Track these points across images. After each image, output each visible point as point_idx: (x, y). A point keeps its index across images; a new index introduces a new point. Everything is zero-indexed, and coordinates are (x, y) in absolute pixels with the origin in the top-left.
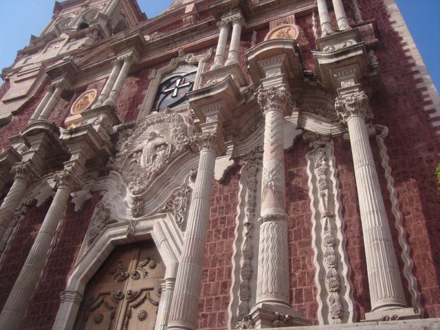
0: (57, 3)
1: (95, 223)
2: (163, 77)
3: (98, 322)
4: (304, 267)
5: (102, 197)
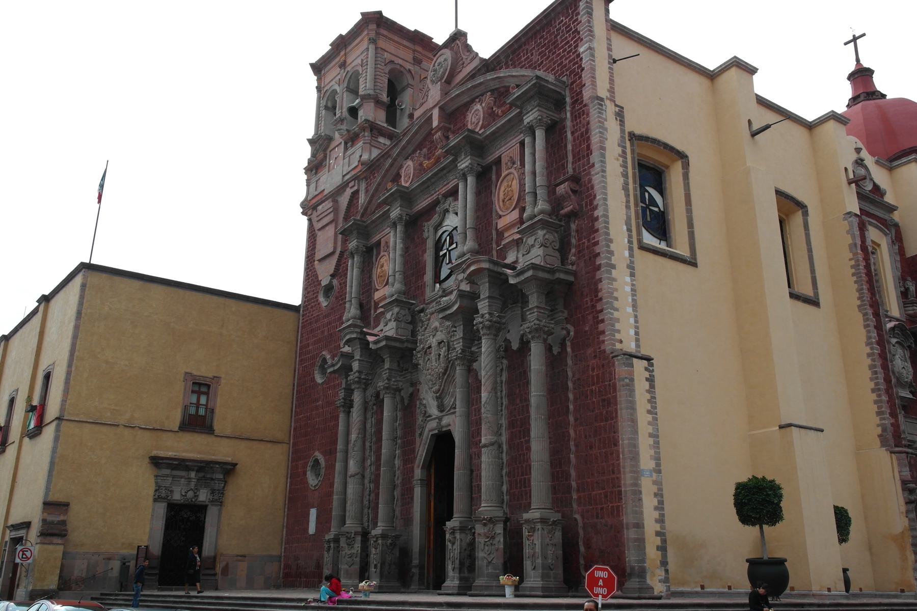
0: (312, 65)
1: (420, 418)
5: (418, 390)
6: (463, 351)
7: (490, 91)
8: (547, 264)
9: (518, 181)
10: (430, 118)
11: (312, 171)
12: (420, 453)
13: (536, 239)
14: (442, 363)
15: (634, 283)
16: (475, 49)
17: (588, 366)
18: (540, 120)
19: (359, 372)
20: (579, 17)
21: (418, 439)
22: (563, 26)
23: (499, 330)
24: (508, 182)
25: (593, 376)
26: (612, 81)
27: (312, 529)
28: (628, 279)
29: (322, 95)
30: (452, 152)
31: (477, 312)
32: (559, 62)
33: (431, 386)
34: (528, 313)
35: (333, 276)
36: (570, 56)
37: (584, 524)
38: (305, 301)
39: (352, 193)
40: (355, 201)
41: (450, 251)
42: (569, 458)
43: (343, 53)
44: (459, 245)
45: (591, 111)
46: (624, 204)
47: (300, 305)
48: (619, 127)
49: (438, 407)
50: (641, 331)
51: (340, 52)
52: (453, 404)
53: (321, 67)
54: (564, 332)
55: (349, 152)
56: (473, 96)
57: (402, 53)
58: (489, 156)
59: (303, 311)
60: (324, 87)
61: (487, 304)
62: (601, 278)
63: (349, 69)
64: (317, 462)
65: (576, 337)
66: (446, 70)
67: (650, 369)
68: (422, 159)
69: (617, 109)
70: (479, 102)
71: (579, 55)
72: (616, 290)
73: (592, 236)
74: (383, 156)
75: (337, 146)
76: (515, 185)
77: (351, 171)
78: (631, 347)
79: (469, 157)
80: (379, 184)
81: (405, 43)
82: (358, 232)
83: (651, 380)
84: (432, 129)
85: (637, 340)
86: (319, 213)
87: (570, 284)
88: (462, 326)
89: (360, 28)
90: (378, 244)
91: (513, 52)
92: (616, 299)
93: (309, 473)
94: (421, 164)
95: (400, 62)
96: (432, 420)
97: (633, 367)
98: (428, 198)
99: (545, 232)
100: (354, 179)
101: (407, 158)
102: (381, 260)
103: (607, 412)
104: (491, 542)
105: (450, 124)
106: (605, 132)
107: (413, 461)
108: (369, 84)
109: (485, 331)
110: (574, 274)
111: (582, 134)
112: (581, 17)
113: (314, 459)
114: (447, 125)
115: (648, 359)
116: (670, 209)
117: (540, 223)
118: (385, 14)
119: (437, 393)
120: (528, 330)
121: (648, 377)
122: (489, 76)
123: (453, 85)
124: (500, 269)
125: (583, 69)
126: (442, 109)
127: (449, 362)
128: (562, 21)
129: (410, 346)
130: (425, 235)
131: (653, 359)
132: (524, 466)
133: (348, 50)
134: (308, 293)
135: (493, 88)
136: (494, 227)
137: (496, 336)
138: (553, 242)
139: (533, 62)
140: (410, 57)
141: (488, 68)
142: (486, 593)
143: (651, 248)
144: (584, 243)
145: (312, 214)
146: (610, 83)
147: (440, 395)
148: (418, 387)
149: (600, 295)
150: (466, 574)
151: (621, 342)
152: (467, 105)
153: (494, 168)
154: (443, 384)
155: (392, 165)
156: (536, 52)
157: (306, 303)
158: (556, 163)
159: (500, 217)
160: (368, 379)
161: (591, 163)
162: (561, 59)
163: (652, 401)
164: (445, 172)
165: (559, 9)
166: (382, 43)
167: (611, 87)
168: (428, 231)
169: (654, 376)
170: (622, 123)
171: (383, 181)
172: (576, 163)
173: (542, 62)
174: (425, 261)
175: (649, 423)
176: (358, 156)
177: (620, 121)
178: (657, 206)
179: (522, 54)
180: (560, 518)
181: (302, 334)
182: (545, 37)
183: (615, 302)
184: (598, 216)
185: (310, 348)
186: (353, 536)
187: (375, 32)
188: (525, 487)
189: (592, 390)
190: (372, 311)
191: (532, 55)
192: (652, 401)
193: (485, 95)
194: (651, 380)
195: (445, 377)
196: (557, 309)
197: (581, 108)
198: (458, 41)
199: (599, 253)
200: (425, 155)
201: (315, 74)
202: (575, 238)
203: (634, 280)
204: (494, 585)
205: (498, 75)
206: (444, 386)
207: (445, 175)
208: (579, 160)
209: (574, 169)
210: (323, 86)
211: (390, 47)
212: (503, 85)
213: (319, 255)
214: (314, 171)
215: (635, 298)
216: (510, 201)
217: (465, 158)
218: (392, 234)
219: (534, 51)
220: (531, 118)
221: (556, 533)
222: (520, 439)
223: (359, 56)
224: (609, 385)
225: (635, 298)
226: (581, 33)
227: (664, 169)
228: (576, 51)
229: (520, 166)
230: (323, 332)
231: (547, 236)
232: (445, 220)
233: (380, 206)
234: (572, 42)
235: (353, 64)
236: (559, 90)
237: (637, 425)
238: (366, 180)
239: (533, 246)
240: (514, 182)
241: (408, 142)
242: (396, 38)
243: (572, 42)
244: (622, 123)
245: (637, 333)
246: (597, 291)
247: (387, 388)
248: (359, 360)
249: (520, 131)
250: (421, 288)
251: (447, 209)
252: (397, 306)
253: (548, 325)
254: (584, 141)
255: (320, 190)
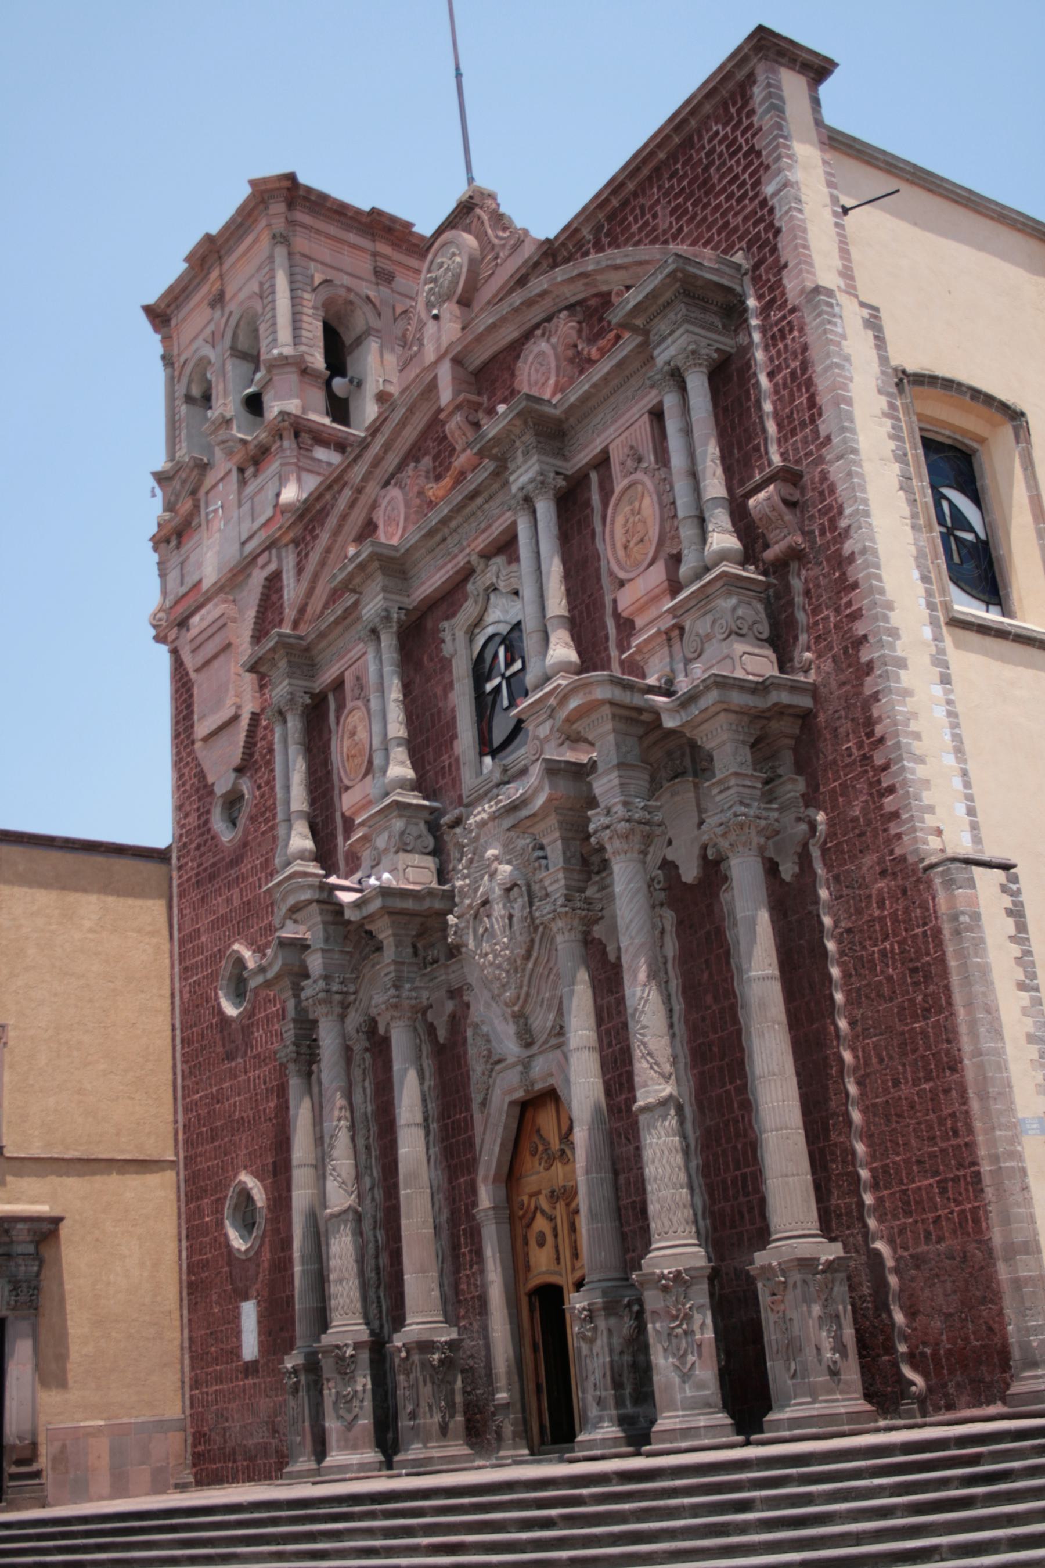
0: (148, 310)
1: (477, 1068)
2: (471, 639)
3: (541, 1244)
4: (746, 1136)
5: (467, 1005)
6: (568, 899)
7: (567, 308)
8: (748, 674)
9: (655, 498)
10: (432, 387)
11: (168, 541)
12: (486, 1147)
13: (714, 622)
14: (518, 933)
15: (952, 697)
16: (519, 223)
17: (869, 896)
18: (693, 352)
19: (327, 978)
20: (755, 119)
21: (477, 1117)
22: (720, 143)
23: (648, 839)
24: (631, 503)
25: (882, 919)
26: (845, 253)
27: (250, 1347)
28: (938, 690)
29: (176, 373)
30: (494, 451)
31: (592, 802)
32: (721, 223)
33: (496, 992)
34: (715, 791)
35: (240, 770)
36: (745, 207)
37: (898, 1260)
38: (181, 836)
39: (266, 579)
40: (274, 597)
41: (508, 680)
42: (847, 1115)
43: (214, 274)
44: (533, 660)
45: (808, 319)
46: (909, 521)
47: (169, 847)
48: (874, 352)
49: (519, 1035)
50: (978, 804)
51: (208, 274)
52: (553, 1027)
53: (168, 312)
54: (804, 827)
55: (250, 489)
56: (529, 325)
57: (349, 260)
58: (580, 452)
59: (178, 859)
60: (179, 355)
61: (616, 781)
62: (877, 693)
63: (232, 306)
64: (245, 1196)
65: (831, 835)
66: (459, 275)
67: (1011, 888)
68: (421, 481)
69: (866, 313)
70: (543, 335)
71: (764, 203)
72: (915, 715)
73: (845, 600)
74: (330, 487)
75: (222, 479)
76: (649, 507)
77: (260, 529)
78: (962, 844)
79: (535, 458)
80: (328, 551)
81: (352, 237)
82: (289, 662)
83: (1016, 913)
84: (440, 410)
85: (974, 827)
86: (194, 632)
87: (806, 717)
88: (559, 843)
89: (249, 214)
90: (339, 685)
91: (611, 217)
92: (917, 736)
93: (227, 1223)
94: (421, 493)
95: (346, 280)
96: (506, 1068)
97: (974, 887)
98: (446, 564)
99: (734, 601)
100: (268, 548)
101: (387, 484)
102: (349, 720)
103: (926, 996)
104: (685, 1326)
105: (479, 394)
106: (847, 364)
107: (470, 1166)
108: (284, 334)
109: (617, 843)
110: (813, 691)
111: (793, 373)
112: (761, 119)
113: (238, 1189)
114: (474, 398)
115: (1006, 867)
116: (1001, 533)
117: (720, 584)
118: (303, 179)
119: (514, 1005)
120: (719, 831)
121: (1010, 906)
122: (561, 273)
123: (477, 306)
124: (637, 700)
125: (778, 231)
126: (457, 361)
127: (536, 928)
128: (717, 133)
129: (438, 905)
130: (447, 649)
131: (1014, 866)
132: (740, 1146)
133: (226, 267)
134: (186, 816)
135: (573, 300)
136: (609, 610)
137: (644, 853)
138: (755, 623)
139: (660, 231)
140: (365, 266)
141: (554, 260)
142: (684, 1445)
143: (973, 620)
144: (827, 618)
145: (177, 638)
146: (842, 258)
147: (523, 1007)
148: (465, 998)
149: (879, 730)
150: (630, 1409)
151: (939, 832)
152: (515, 349)
153: (594, 477)
154: (526, 982)
155: (352, 504)
156: (664, 208)
157: (184, 840)
158: (740, 449)
159: (622, 584)
160: (346, 993)
161: (823, 434)
162: (723, 215)
163: (1026, 959)
164: (479, 500)
165: (707, 108)
166: (301, 242)
167: (844, 266)
168: (454, 640)
169: (1021, 904)
170: (880, 341)
171: (335, 541)
172: (786, 441)
173: (680, 229)
174: (453, 710)
175: (1025, 1011)
176: (271, 495)
177: (876, 337)
178: (971, 529)
179: (631, 219)
180: (841, 1254)
181: (180, 911)
182: (681, 173)
183: (916, 743)
184: (853, 553)
185: (203, 939)
186: (349, 1352)
187: (283, 220)
188: (746, 1194)
189: (883, 953)
190: (340, 839)
191: (655, 216)
192: (1026, 959)
193: (555, 320)
194: (1016, 913)
195: (530, 965)
196: (780, 776)
197: (784, 317)
198: (478, 211)
199: (865, 637)
200: (427, 472)
201: (157, 329)
202: (805, 610)
203: (952, 691)
204: (702, 1424)
205: (582, 270)
206: (529, 987)
207: (480, 507)
208: (793, 432)
209: (784, 456)
210: (175, 352)
211: (323, 250)
212: (594, 291)
213: (201, 729)
214: (174, 543)
215: (957, 731)
216: (640, 545)
217: (525, 462)
218: (370, 656)
219: (658, 208)
220: (672, 351)
221: (836, 1289)
222: (724, 1085)
223: (253, 276)
224: (925, 932)
225: (957, 731)
226: (764, 153)
227: (975, 445)
228: (756, 196)
229: (657, 462)
230: (229, 901)
231: (740, 612)
232: (490, 610)
233: (335, 595)
234: (746, 176)
235: (242, 296)
236: (725, 281)
237: (998, 1019)
238: (297, 545)
239: (709, 637)
240: (647, 501)
241: (387, 447)
242: (332, 230)
243: (746, 176)
244: (880, 341)
245: (971, 812)
246: (870, 723)
247: (395, 1006)
248: (323, 950)
249: (648, 383)
250: (451, 771)
251: (492, 584)
252: (401, 816)
253: (765, 814)
254: (799, 389)
255: (190, 582)
